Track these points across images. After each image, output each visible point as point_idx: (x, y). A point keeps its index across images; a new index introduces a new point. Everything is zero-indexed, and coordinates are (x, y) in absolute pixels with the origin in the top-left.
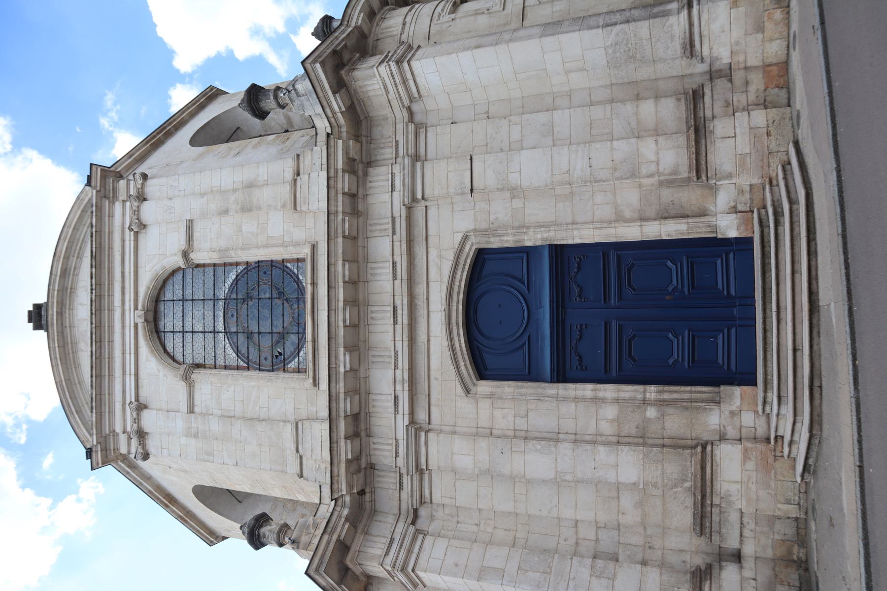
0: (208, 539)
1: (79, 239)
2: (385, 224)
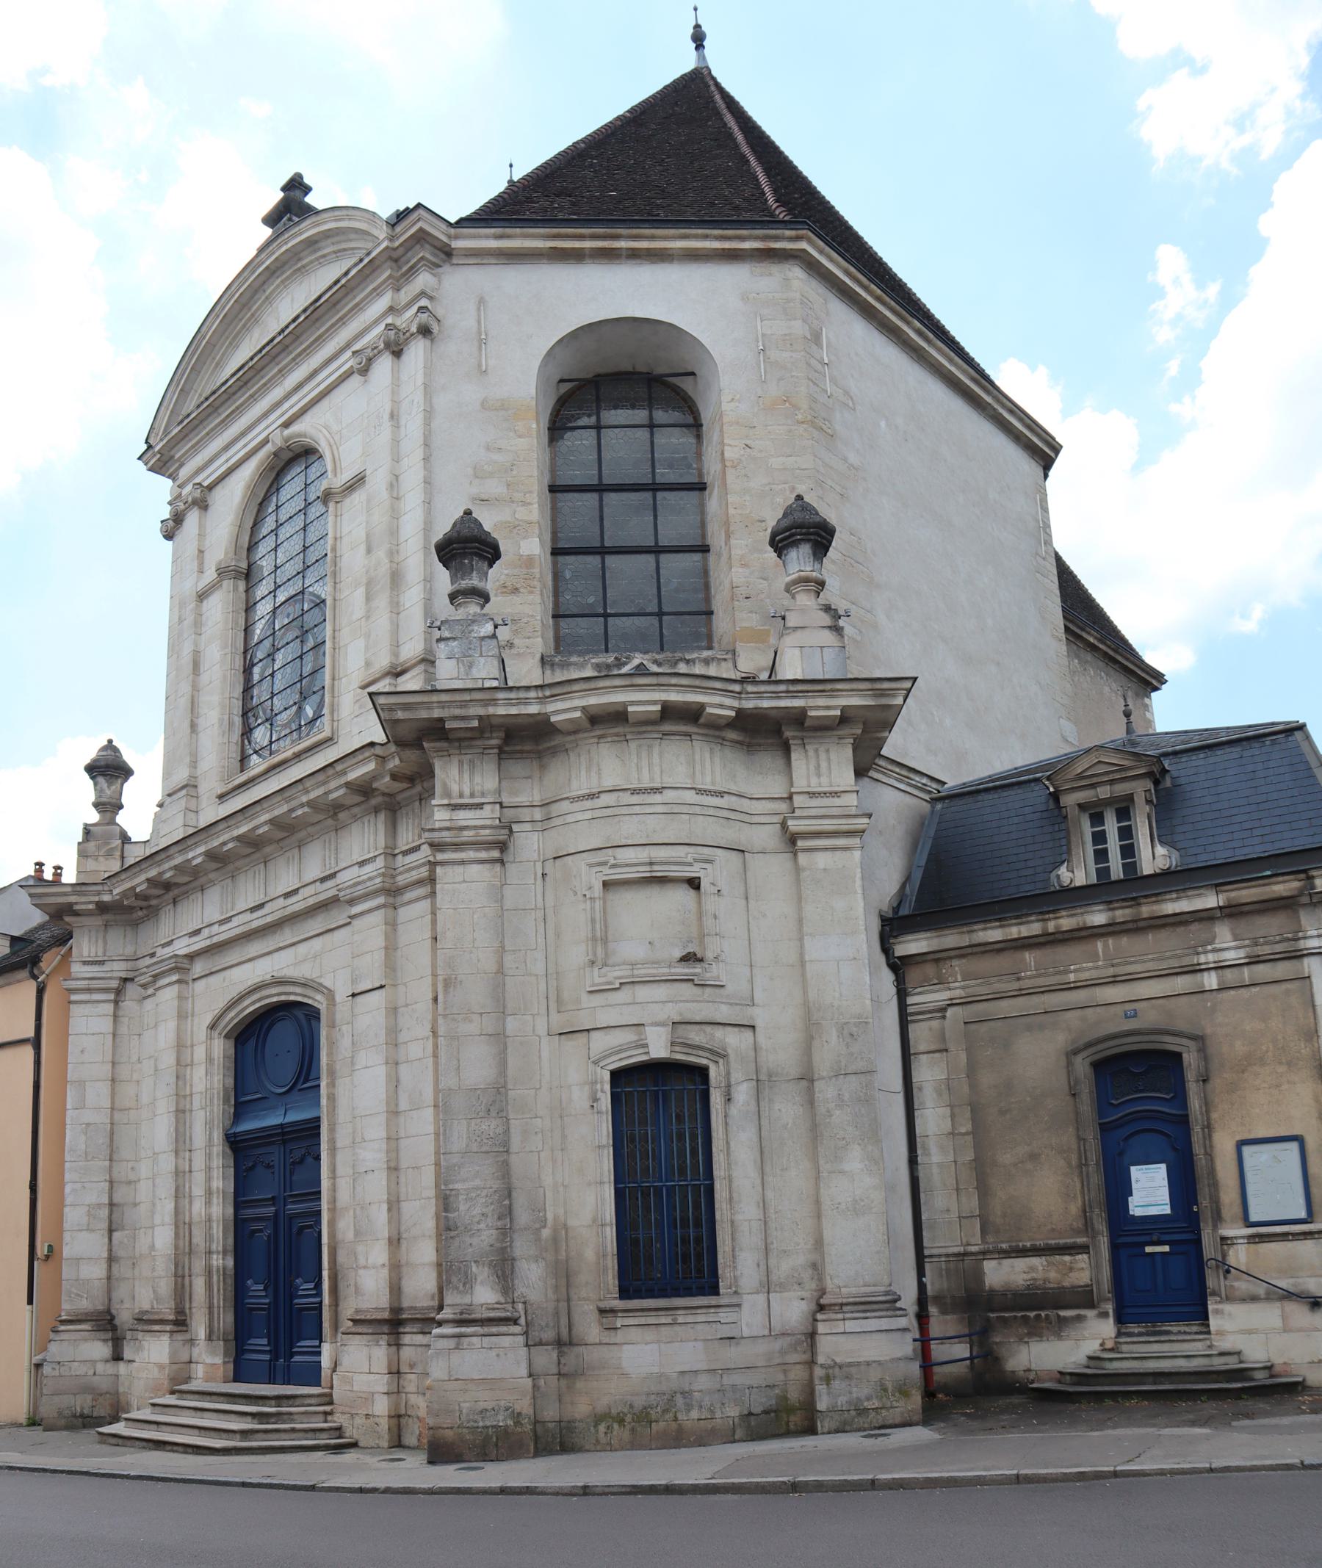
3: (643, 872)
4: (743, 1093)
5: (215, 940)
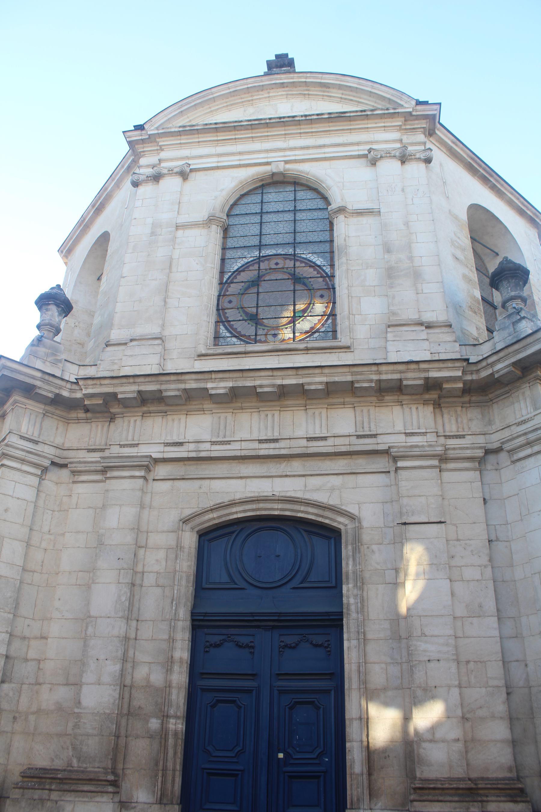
0: (64, 249)
1: (361, 98)
2: (370, 427)
5: (203, 454)
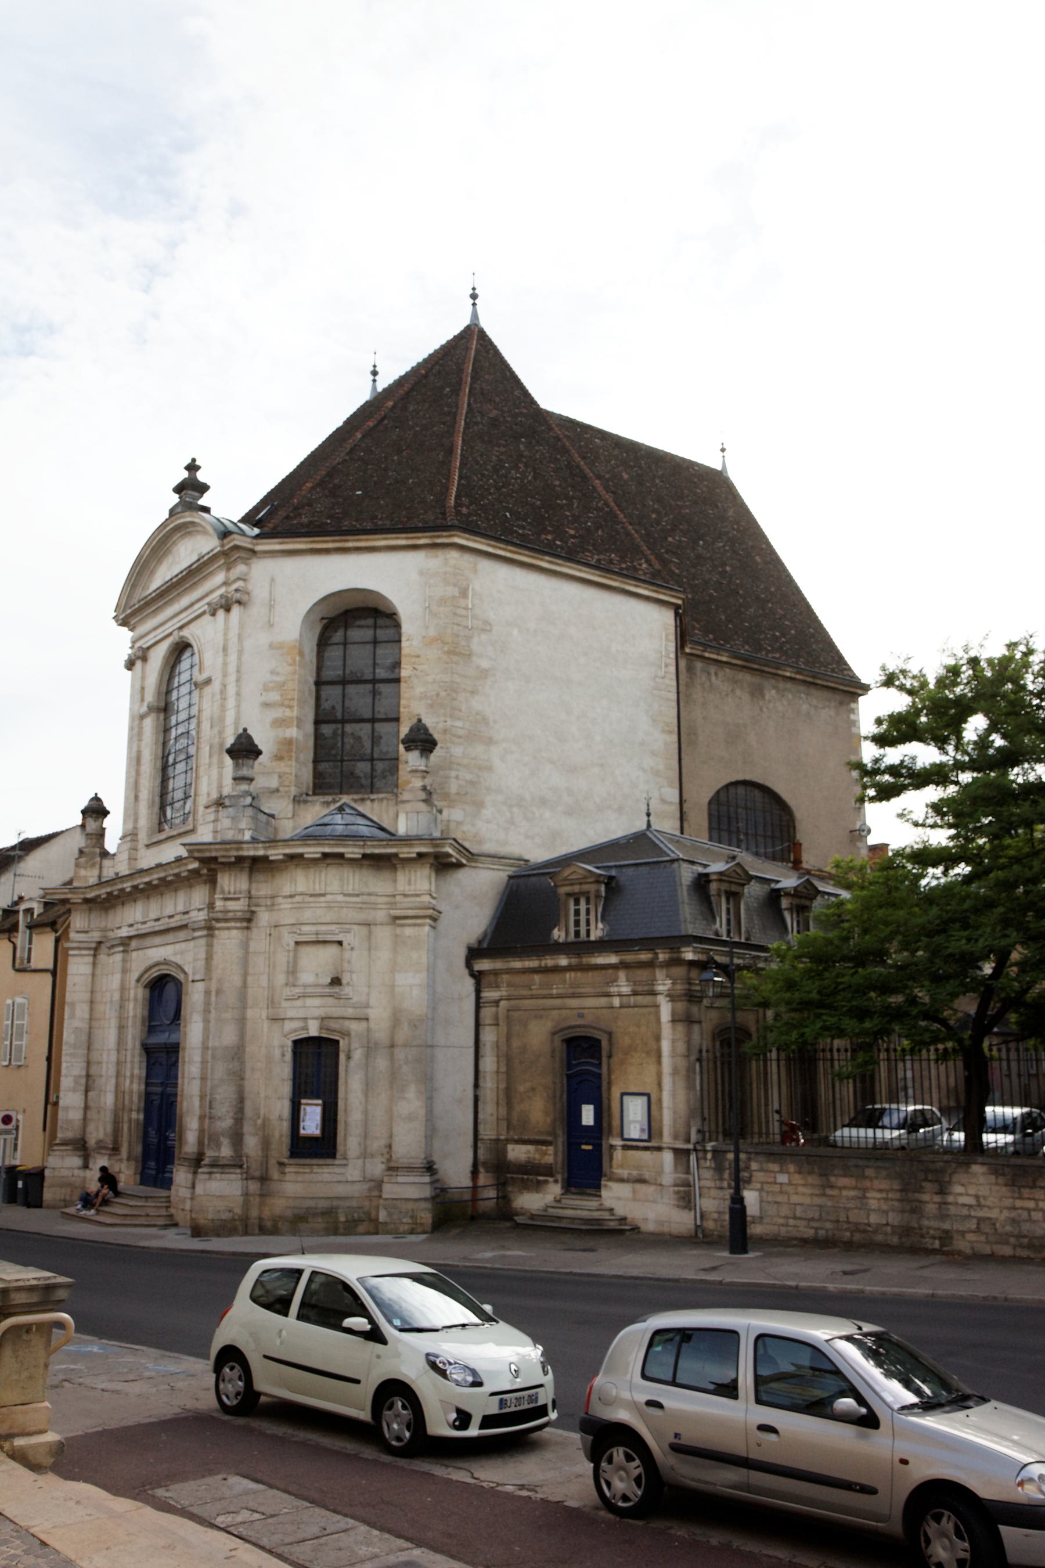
3: (313, 938)
4: (358, 1055)
